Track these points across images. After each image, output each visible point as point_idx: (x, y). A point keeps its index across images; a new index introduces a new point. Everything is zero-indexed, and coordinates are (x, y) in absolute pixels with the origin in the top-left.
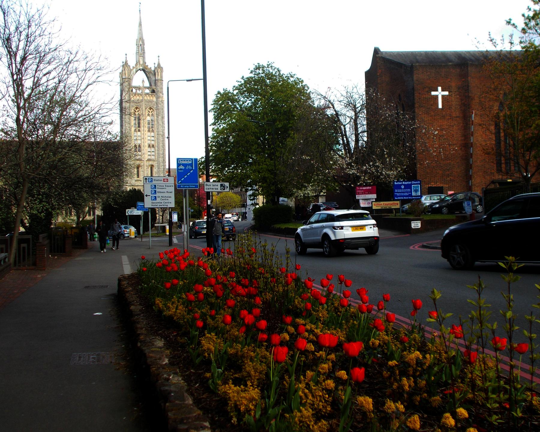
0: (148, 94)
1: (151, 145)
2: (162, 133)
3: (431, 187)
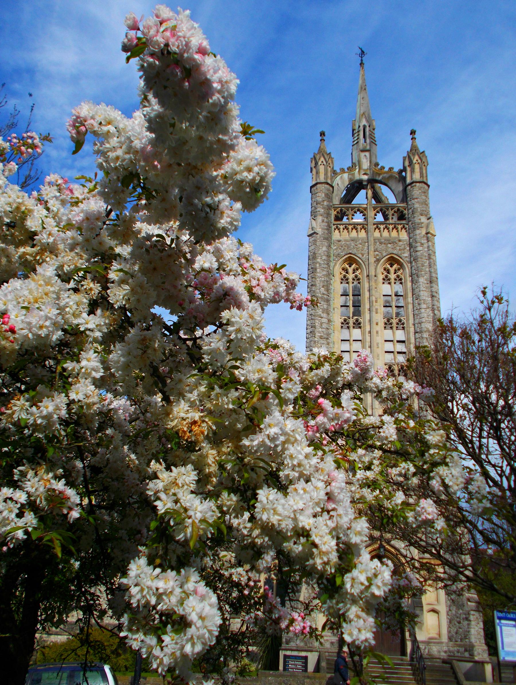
1: (396, 368)
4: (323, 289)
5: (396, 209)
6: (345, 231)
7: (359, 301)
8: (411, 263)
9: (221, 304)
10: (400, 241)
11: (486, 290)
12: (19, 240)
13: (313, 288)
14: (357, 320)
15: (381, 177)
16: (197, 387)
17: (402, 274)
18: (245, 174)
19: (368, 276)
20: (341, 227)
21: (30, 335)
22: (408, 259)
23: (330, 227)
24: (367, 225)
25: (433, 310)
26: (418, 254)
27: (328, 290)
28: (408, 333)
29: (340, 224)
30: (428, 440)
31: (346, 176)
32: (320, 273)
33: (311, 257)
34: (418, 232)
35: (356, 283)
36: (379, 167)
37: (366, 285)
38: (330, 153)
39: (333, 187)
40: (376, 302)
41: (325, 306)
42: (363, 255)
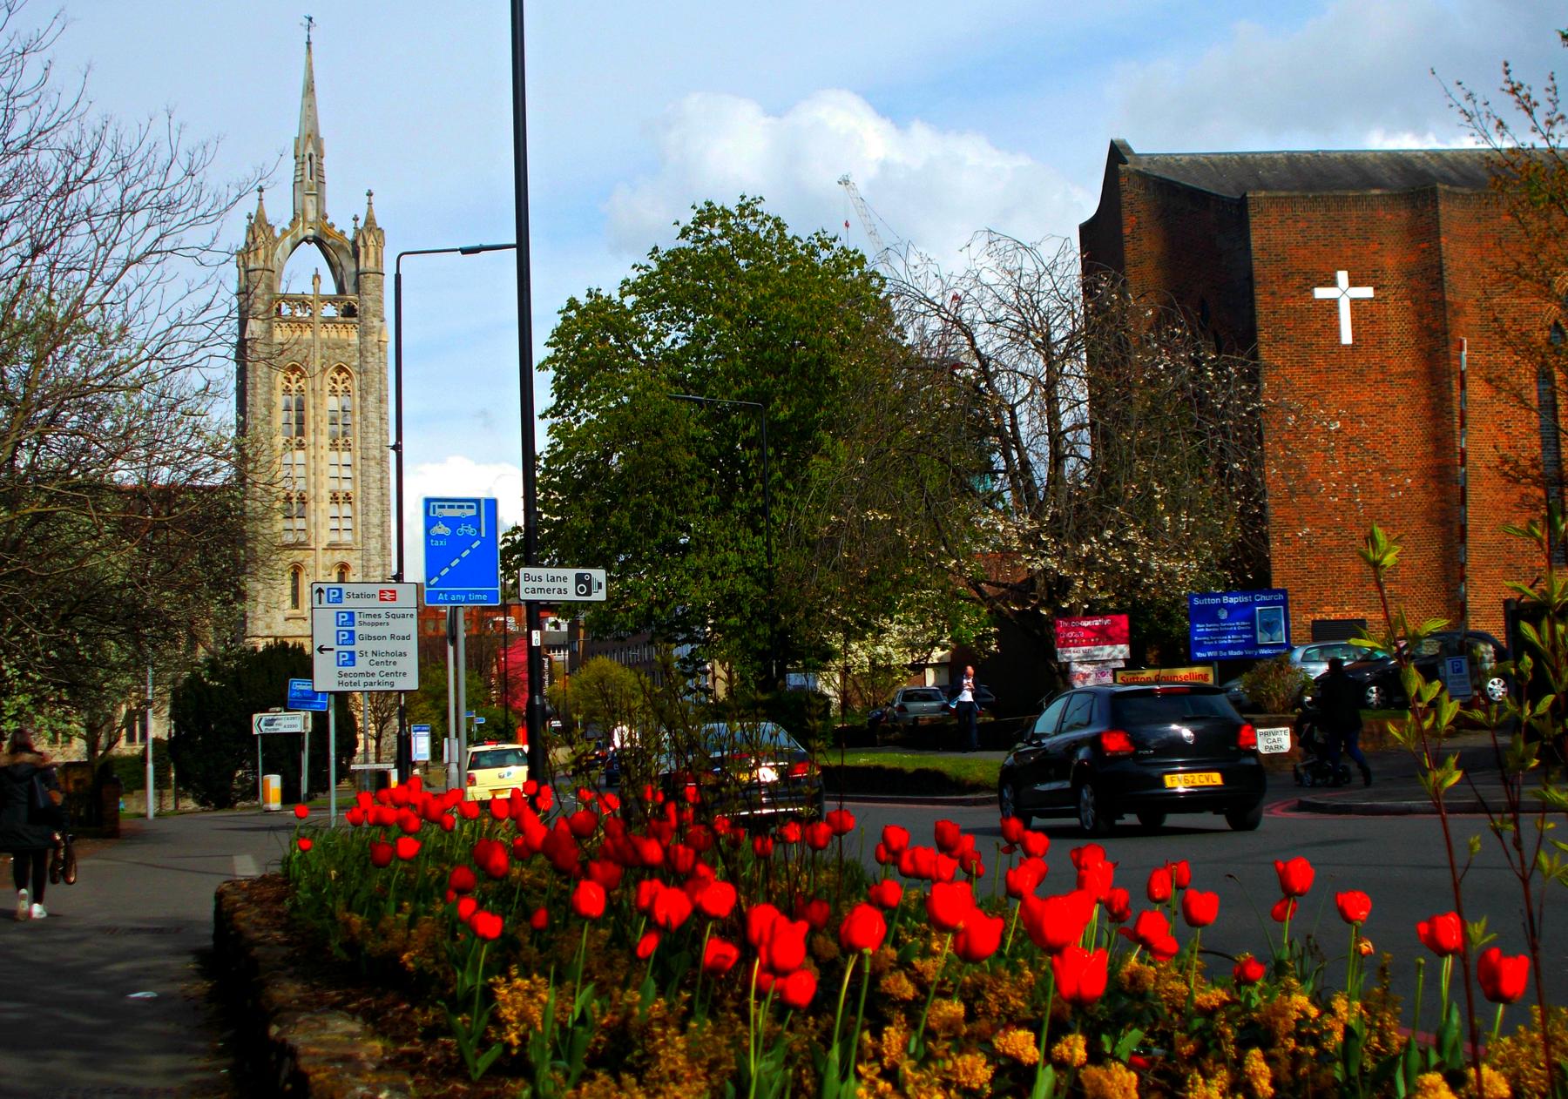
0: (330, 320)
1: (341, 496)
2: (377, 453)
3: (1323, 621)
34: (369, 338)
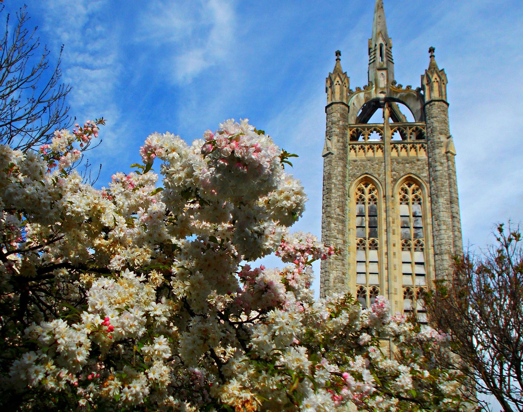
4: (338, 210)
5: (414, 128)
6: (361, 151)
7: (375, 222)
8: (430, 183)
9: (263, 296)
10: (418, 160)
11: (503, 227)
12: (94, 232)
13: (329, 209)
14: (373, 241)
15: (399, 95)
16: (247, 370)
17: (420, 194)
18: (285, 202)
19: (385, 196)
20: (357, 147)
21: (124, 333)
22: (427, 179)
23: (346, 147)
24: (384, 144)
25: (453, 231)
26: (438, 173)
27: (343, 211)
28: (427, 256)
29: (356, 144)
30: (442, 390)
31: (362, 95)
32: (335, 194)
33: (326, 178)
34: (437, 151)
35: (372, 203)
36: (397, 85)
37: (383, 206)
38: (346, 73)
39: (348, 107)
40: (393, 223)
41: (341, 227)
42: (379, 175)
